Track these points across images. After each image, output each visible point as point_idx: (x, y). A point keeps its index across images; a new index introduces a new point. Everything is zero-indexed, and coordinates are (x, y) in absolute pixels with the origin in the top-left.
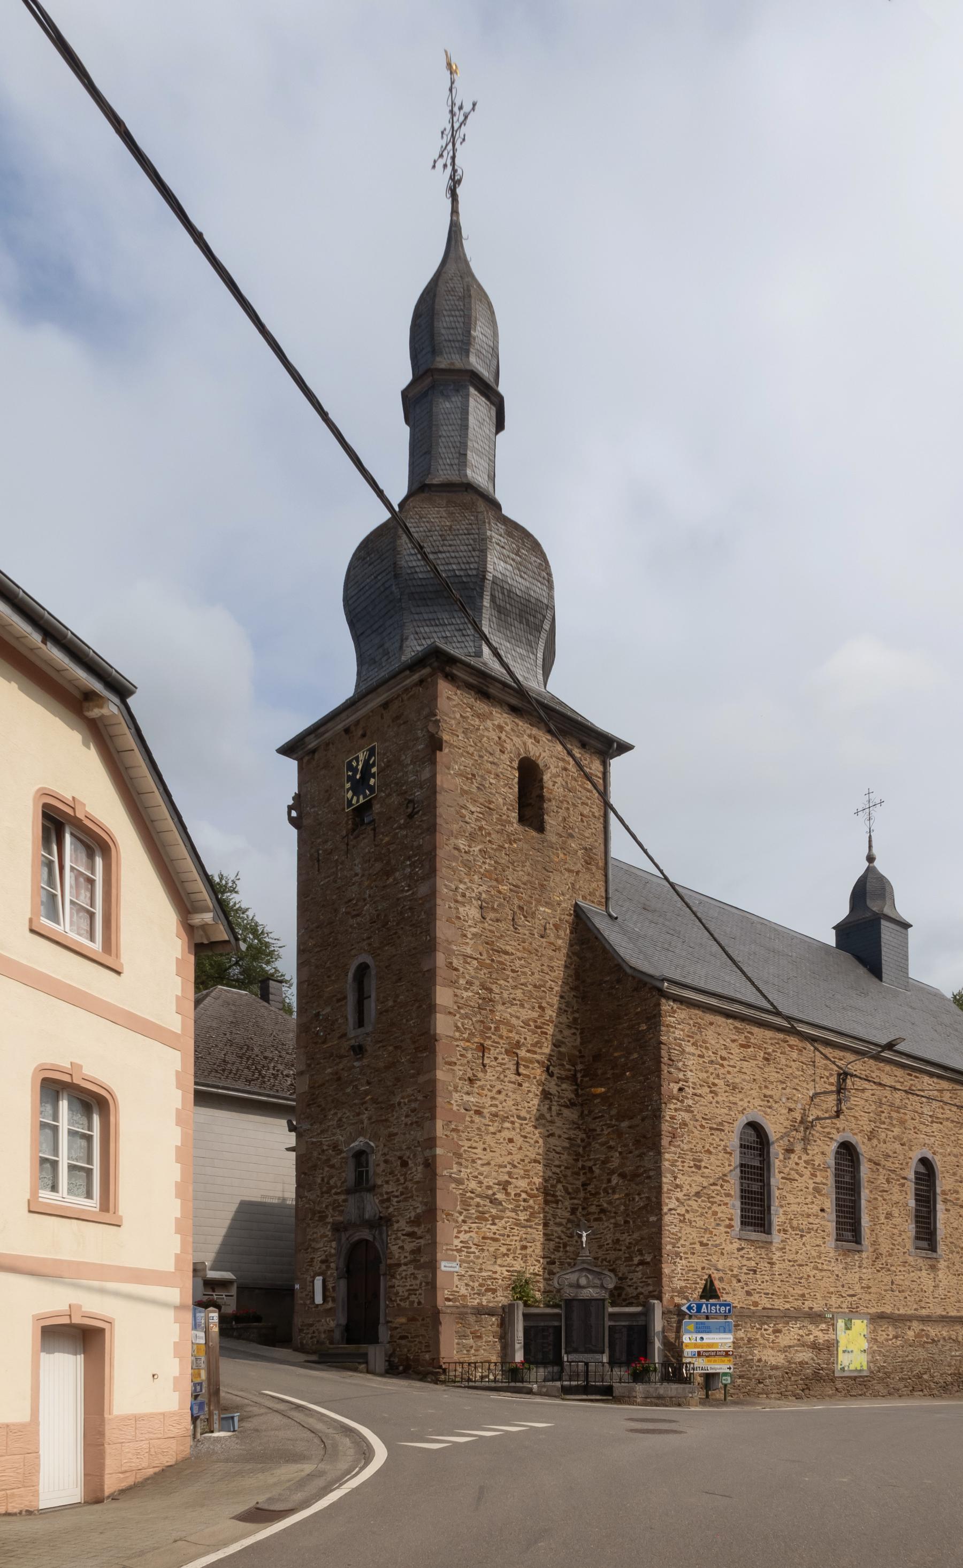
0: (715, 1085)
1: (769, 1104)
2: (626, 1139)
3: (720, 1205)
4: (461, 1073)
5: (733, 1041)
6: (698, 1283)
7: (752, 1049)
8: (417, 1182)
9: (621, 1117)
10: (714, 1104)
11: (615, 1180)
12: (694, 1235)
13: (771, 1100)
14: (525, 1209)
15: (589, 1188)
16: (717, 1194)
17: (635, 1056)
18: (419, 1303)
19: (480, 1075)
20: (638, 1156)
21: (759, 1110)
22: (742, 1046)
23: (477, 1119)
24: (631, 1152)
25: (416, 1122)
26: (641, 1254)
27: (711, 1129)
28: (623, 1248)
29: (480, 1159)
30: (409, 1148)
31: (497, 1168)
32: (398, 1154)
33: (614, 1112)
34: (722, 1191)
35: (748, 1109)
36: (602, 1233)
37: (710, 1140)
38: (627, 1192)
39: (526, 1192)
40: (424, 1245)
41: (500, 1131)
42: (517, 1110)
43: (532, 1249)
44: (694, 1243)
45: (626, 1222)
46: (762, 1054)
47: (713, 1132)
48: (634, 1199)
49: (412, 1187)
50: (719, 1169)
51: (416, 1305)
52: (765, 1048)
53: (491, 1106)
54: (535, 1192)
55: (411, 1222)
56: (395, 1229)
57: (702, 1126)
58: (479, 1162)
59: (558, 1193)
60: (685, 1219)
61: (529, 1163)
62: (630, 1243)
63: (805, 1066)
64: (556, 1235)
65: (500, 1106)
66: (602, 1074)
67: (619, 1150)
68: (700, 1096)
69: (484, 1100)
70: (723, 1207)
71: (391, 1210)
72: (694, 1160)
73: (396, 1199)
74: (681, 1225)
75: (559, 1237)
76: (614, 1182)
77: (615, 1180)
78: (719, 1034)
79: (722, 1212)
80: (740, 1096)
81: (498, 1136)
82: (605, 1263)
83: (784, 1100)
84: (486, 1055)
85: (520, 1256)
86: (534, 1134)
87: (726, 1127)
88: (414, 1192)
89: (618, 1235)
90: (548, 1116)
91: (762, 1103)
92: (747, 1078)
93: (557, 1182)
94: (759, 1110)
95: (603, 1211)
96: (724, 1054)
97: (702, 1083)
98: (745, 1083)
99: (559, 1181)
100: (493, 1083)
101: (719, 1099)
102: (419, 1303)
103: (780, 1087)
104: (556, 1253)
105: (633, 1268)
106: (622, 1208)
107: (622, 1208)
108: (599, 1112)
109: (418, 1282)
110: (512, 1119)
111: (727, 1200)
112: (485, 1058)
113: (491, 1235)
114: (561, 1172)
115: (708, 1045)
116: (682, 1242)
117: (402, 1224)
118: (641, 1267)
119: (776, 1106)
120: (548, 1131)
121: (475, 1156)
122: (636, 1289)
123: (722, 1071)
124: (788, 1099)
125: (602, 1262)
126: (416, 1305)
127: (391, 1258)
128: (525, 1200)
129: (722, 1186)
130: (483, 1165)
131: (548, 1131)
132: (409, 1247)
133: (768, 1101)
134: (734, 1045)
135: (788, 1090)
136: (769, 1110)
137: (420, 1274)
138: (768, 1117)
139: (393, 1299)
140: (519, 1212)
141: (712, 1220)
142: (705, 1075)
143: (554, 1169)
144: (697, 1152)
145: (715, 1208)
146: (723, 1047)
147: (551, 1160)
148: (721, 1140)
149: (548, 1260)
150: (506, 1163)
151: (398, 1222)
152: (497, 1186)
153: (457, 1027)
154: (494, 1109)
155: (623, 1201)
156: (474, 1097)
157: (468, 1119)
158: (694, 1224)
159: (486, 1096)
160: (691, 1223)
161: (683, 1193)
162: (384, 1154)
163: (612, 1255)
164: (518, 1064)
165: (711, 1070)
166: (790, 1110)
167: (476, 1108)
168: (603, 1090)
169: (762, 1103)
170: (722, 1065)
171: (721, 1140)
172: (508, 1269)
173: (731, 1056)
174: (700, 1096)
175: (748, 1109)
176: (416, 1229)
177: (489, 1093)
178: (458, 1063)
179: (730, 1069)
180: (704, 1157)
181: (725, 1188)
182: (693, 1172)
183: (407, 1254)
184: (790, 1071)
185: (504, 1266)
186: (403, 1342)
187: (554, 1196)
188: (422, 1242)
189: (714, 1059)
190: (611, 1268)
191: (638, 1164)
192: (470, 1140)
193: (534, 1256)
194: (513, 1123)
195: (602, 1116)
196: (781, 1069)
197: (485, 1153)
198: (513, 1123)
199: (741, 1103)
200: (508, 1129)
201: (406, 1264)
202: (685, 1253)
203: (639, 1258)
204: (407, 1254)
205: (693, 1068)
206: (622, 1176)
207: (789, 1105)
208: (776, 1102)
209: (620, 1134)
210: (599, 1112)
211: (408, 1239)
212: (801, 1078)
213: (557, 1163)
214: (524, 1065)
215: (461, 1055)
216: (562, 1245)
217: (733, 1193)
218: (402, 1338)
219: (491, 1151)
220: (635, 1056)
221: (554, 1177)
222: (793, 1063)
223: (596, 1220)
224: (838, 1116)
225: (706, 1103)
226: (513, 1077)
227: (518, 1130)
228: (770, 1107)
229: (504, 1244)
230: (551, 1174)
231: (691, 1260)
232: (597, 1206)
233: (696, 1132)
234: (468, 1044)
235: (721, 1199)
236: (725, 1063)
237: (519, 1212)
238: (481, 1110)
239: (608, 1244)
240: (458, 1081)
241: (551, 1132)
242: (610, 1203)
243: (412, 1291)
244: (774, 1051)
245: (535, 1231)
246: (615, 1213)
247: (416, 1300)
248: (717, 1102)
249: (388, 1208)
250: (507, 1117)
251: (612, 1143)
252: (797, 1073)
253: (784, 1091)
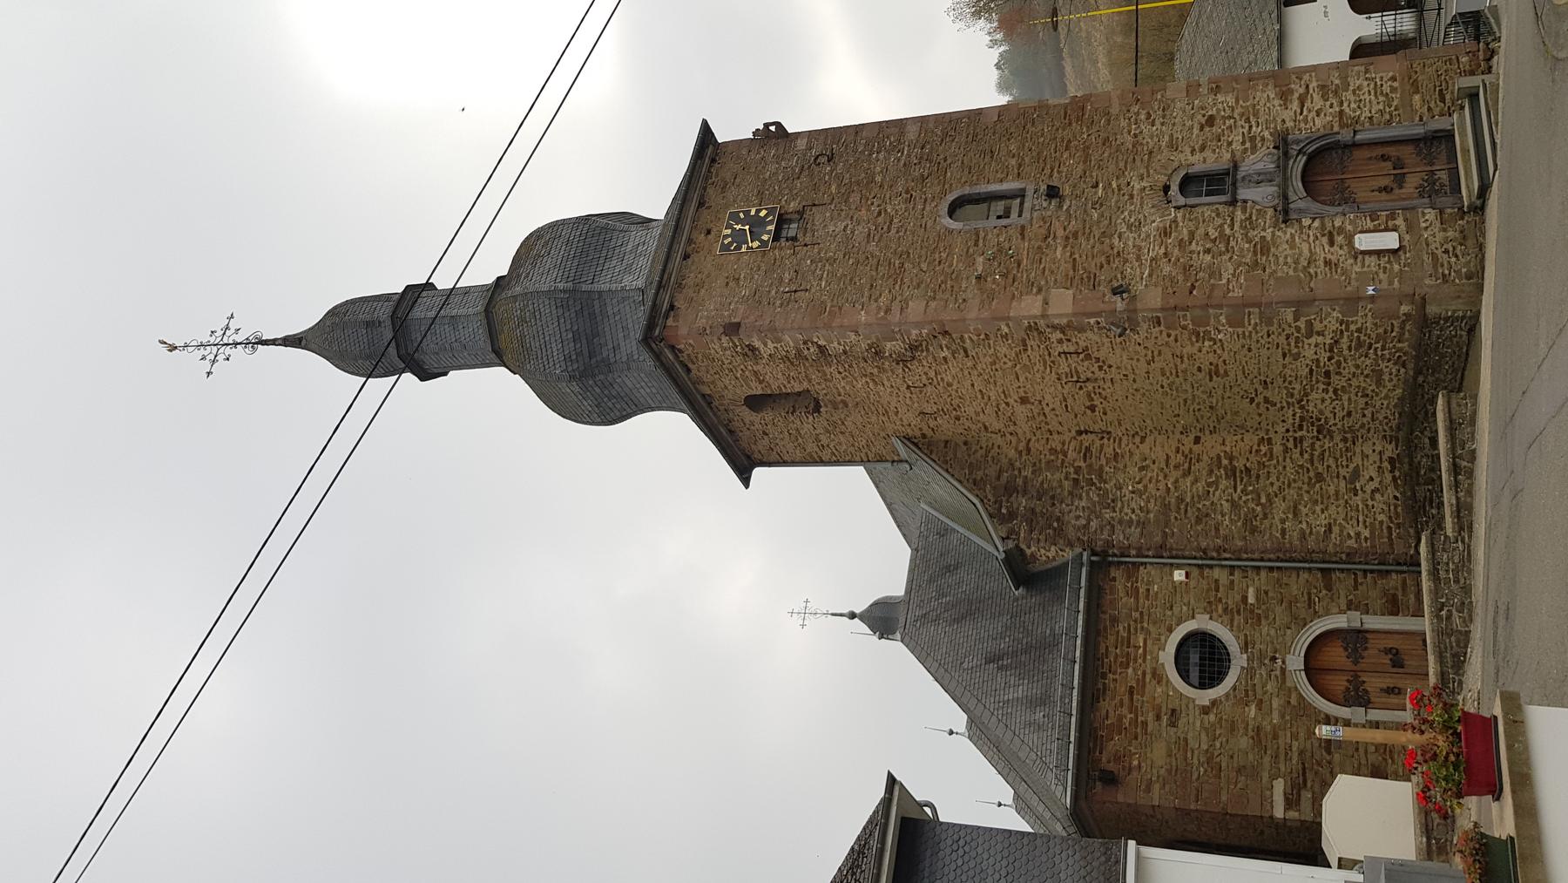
18: (1393, 79)
30: (1192, 117)
32: (1196, 131)
40: (1317, 81)
49: (1241, 106)
51: (1396, 84)
56: (1292, 124)
71: (1266, 134)
73: (1254, 129)
88: (1248, 104)
102: (1393, 79)
109: (1366, 83)
117: (1287, 115)
126: (1396, 84)
127: (1332, 126)
132: (1318, 103)
137: (1354, 82)
139: (1388, 117)
151: (1283, 121)
162: (1193, 151)
176: (1296, 95)
183: (1328, 103)
186: (1448, 97)
188: (1314, 84)
201: (1341, 103)
204: (1328, 103)
211: (1308, 104)
218: (1443, 100)
243: (1377, 90)
247: (1389, 83)
249: (1263, 139)
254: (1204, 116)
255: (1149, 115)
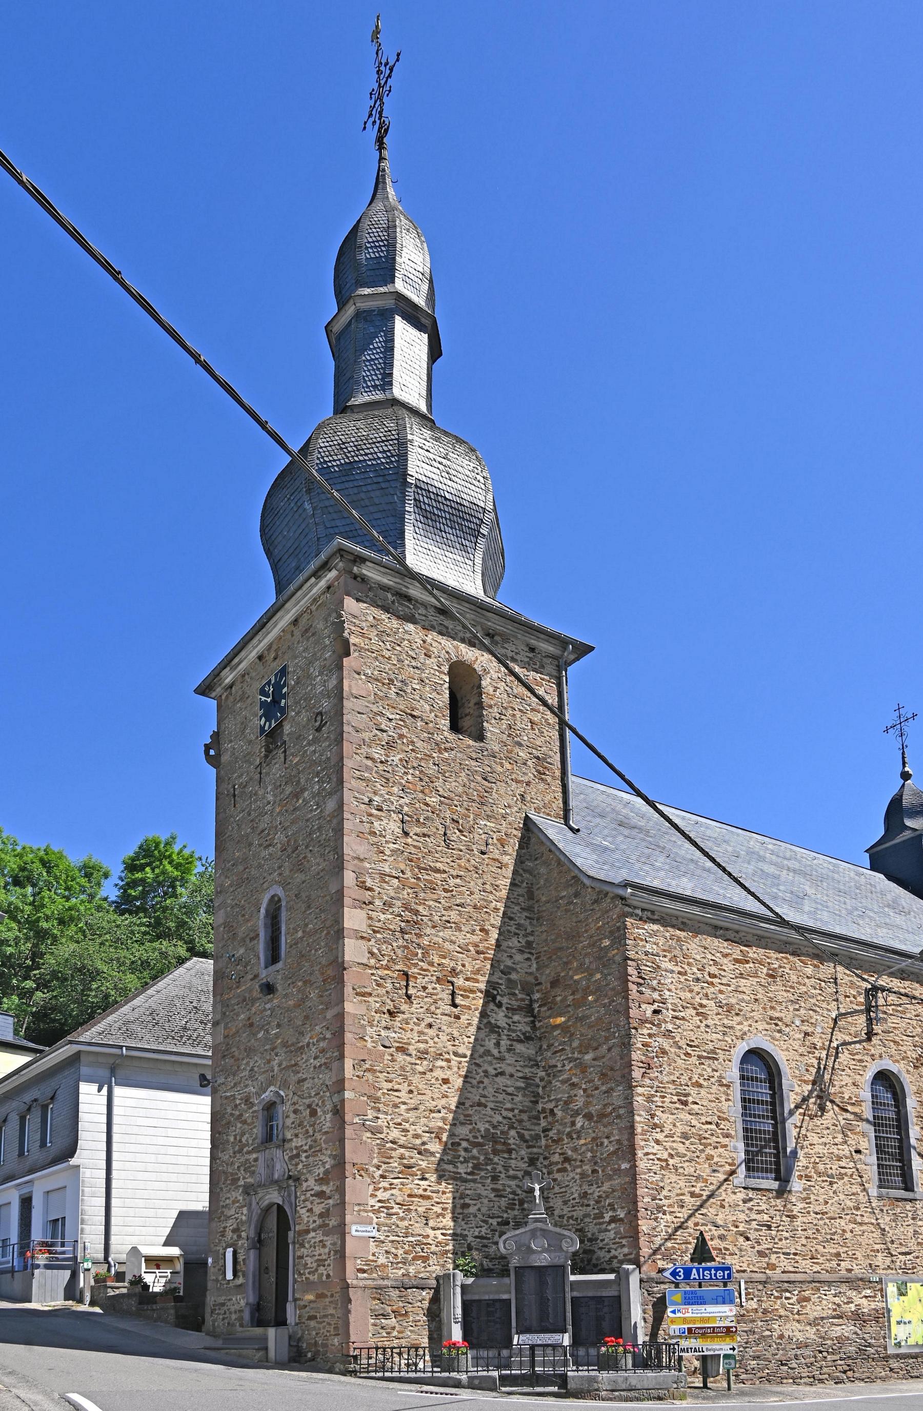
0: (701, 1005)
1: (778, 1028)
2: (591, 1073)
3: (716, 1148)
4: (378, 1005)
5: (725, 956)
6: (690, 1243)
7: (751, 965)
8: (326, 1133)
9: (584, 1048)
10: (703, 1029)
11: (580, 1122)
12: (682, 1184)
13: (780, 1023)
14: (466, 1161)
15: (551, 1134)
16: (712, 1135)
17: (598, 976)
19: (404, 1007)
20: (605, 1093)
21: (765, 1035)
22: (737, 961)
23: (400, 1057)
24: (597, 1089)
25: (325, 1064)
26: (614, 1210)
27: (699, 1057)
28: (592, 1203)
29: (404, 1103)
31: (427, 1113)
33: (576, 1044)
34: (719, 1131)
35: (748, 1034)
36: (567, 1186)
37: (699, 1071)
38: (594, 1135)
39: (467, 1140)
41: (431, 1070)
42: (454, 1045)
43: (476, 1207)
44: (683, 1194)
45: (594, 1171)
46: (765, 970)
47: (703, 1061)
48: (602, 1144)
50: (713, 1104)
52: (769, 963)
53: (419, 1041)
54: (480, 1140)
55: (321, 1181)
57: (687, 1054)
58: (403, 1107)
59: (511, 1141)
60: (668, 1165)
61: (471, 1106)
62: (599, 1197)
63: (823, 984)
64: (509, 1190)
65: (431, 1042)
66: (562, 1001)
67: (584, 1086)
68: (683, 1019)
69: (409, 1034)
70: (721, 1150)
72: (678, 1094)
74: (663, 1172)
75: (514, 1193)
76: (579, 1125)
77: (580, 1122)
78: (705, 948)
79: (720, 1156)
80: (738, 1019)
81: (428, 1076)
82: (571, 1222)
83: (798, 1023)
84: (411, 984)
85: (461, 1216)
86: (478, 1074)
87: (721, 1055)
89: (585, 1187)
90: (495, 1052)
91: (767, 1027)
92: (746, 998)
93: (509, 1129)
94: (765, 1035)
95: (567, 1160)
96: (713, 970)
97: (685, 1004)
98: (744, 1004)
99: (511, 1127)
100: (422, 1016)
101: (710, 1022)
103: (791, 1008)
104: (509, 1211)
105: (604, 1226)
106: (589, 1154)
107: (589, 1154)
108: (559, 1045)
110: (447, 1056)
111: (725, 1141)
112: (410, 988)
113: (421, 1192)
114: (514, 1116)
115: (691, 960)
116: (665, 1193)
118: (613, 1225)
119: (787, 1029)
120: (495, 1069)
121: (397, 1100)
122: (609, 1252)
123: (712, 990)
124: (803, 1021)
125: (568, 1221)
128: (466, 1150)
129: (717, 1125)
130: (409, 1110)
131: (495, 1069)
133: (776, 1025)
134: (725, 961)
135: (802, 1011)
136: (778, 1035)
138: (776, 1043)
140: (459, 1165)
141: (707, 1166)
142: (689, 995)
143: (505, 1113)
144: (681, 1085)
145: (709, 1151)
146: (711, 963)
147: (500, 1102)
148: (714, 1070)
149: (500, 1220)
150: (439, 1107)
152: (427, 1135)
153: (372, 953)
154: (422, 1046)
155: (590, 1146)
156: (395, 1032)
157: (388, 1057)
158: (681, 1170)
159: (412, 1030)
160: (677, 1170)
161: (664, 1134)
163: (579, 1212)
164: (453, 994)
165: (696, 989)
166: (807, 1034)
167: (398, 1045)
168: (563, 1019)
169: (767, 1027)
170: (712, 984)
171: (714, 1070)
172: (444, 1231)
173: (723, 973)
174: (683, 1019)
175: (748, 1034)
177: (416, 1028)
178: (375, 993)
179: (723, 988)
180: (693, 1091)
181: (722, 1126)
182: (677, 1109)
184: (804, 989)
185: (438, 1229)
187: (504, 1144)
189: (700, 976)
190: (579, 1227)
191: (606, 1102)
192: (391, 1081)
193: (480, 1216)
194: (448, 1061)
195: (563, 1050)
196: (793, 988)
197: (411, 1096)
198: (448, 1061)
199: (739, 1027)
200: (441, 1067)
202: (669, 1206)
203: (611, 1213)
205: (672, 987)
206: (588, 1117)
207: (804, 1028)
208: (787, 1026)
209: (583, 1068)
210: (559, 1045)
212: (819, 998)
213: (509, 1106)
214: (462, 995)
215: (378, 985)
216: (517, 1202)
217: (733, 1133)
219: (419, 1094)
220: (598, 976)
221: (505, 1122)
222: (806, 980)
223: (559, 1171)
224: (869, 1039)
225: (691, 1028)
226: (449, 1009)
227: (456, 1069)
228: (780, 1031)
229: (438, 1203)
230: (501, 1119)
231: (679, 1215)
232: (560, 1154)
233: (680, 1062)
234: (386, 972)
235: (718, 1140)
236: (715, 981)
237: (459, 1165)
238: (406, 1046)
239: (574, 1199)
240: (373, 1014)
241: (500, 1070)
242: (575, 1150)
244: (780, 967)
245: (480, 1185)
246: (581, 1161)
248: (707, 1026)
250: (441, 1055)
251: (575, 1080)
252: (813, 991)
253: (797, 1013)
254: (317, 1105)
255: (323, 1051)
